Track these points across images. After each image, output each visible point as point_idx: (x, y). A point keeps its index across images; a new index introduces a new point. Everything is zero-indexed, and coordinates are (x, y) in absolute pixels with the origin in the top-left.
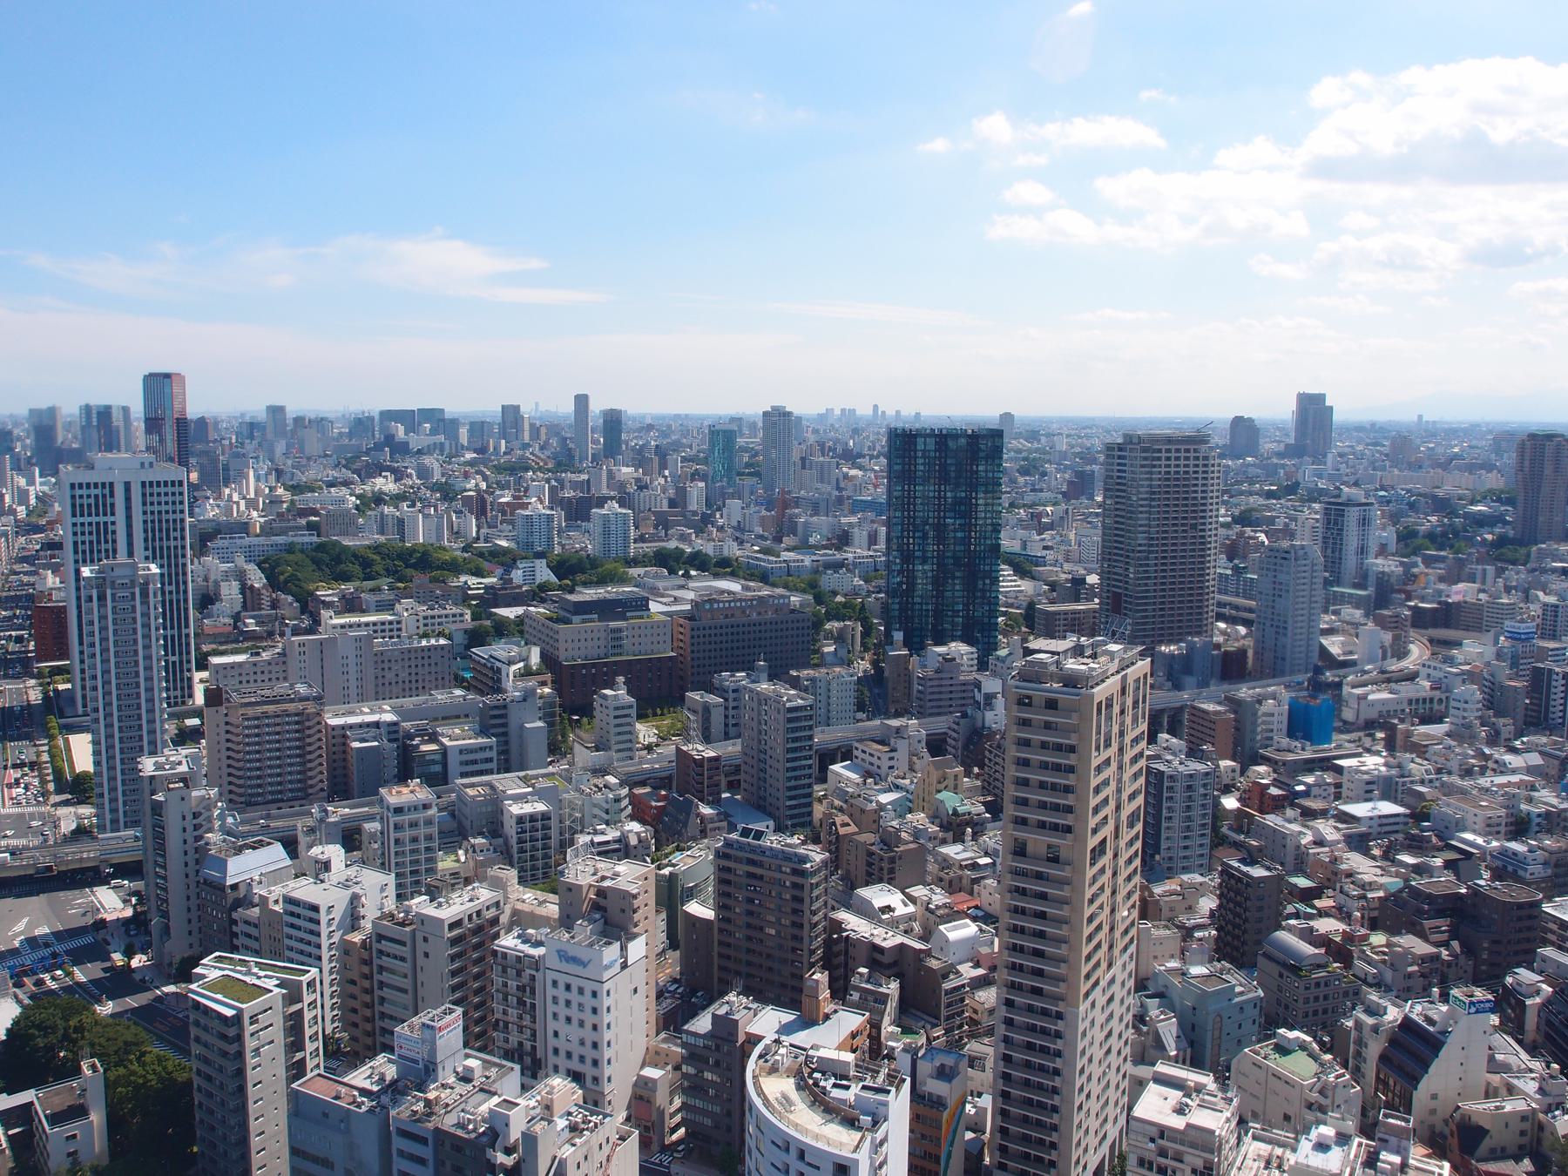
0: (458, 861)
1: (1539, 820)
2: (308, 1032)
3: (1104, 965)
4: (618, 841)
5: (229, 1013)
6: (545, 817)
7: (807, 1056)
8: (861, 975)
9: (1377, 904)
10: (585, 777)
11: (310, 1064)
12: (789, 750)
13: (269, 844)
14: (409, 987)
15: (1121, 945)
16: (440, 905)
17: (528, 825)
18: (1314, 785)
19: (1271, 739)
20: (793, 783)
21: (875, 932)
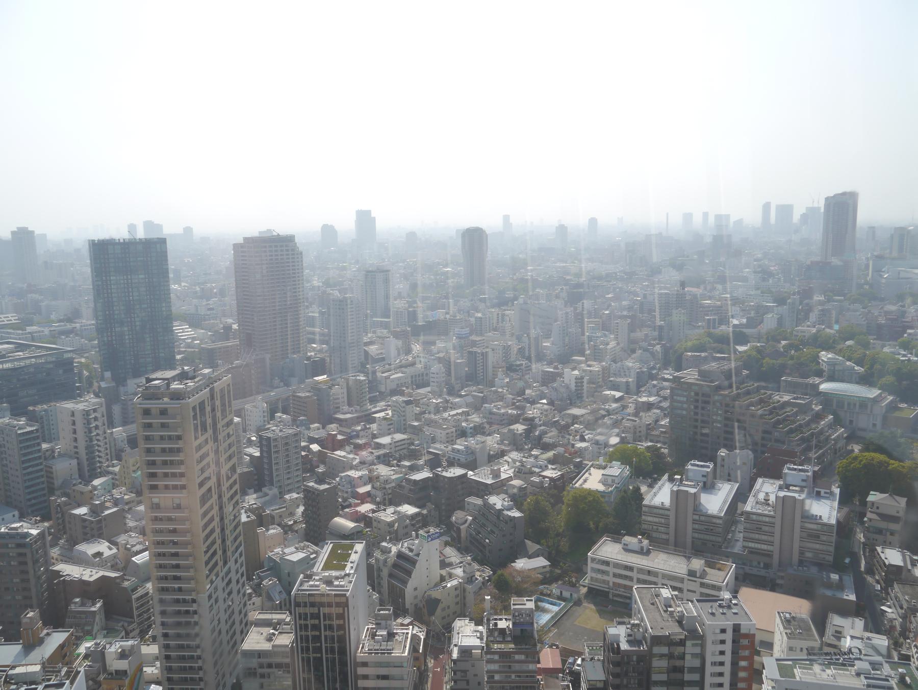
1: (471, 430)
3: (221, 563)
7: (7, 675)
8: (76, 603)
9: (390, 491)
12: (23, 462)
15: (232, 549)
18: (360, 430)
19: (339, 407)
20: (28, 484)
21: (84, 572)
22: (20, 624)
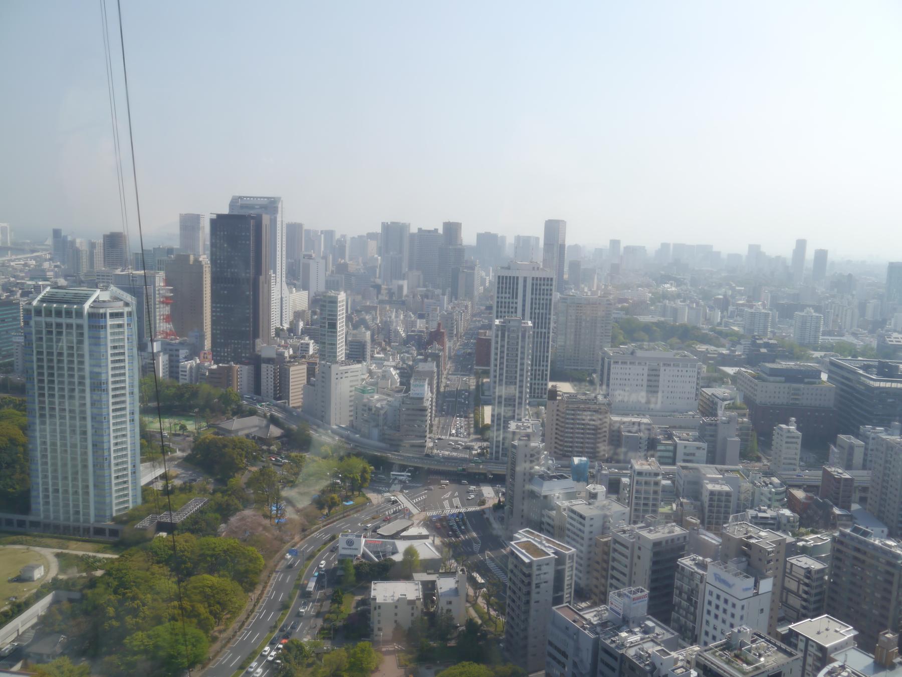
0: (672, 509)
2: (566, 583)
4: (772, 518)
5: (527, 561)
6: (728, 494)
10: (758, 476)
11: (565, 600)
13: (567, 478)
14: (626, 571)
16: (651, 531)
17: (716, 498)
22: (877, 641)
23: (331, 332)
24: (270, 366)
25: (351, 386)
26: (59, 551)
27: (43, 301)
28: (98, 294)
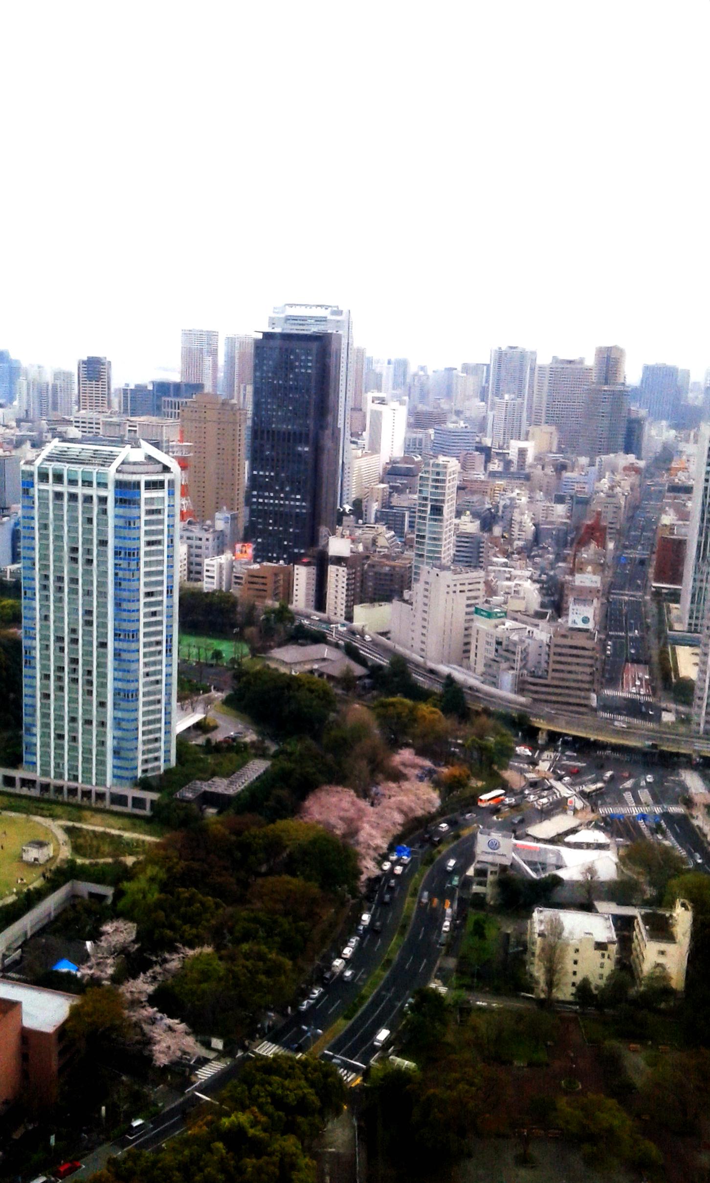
23: (435, 520)
24: (341, 569)
25: (468, 606)
26: (70, 824)
27: (50, 459)
28: (126, 453)
